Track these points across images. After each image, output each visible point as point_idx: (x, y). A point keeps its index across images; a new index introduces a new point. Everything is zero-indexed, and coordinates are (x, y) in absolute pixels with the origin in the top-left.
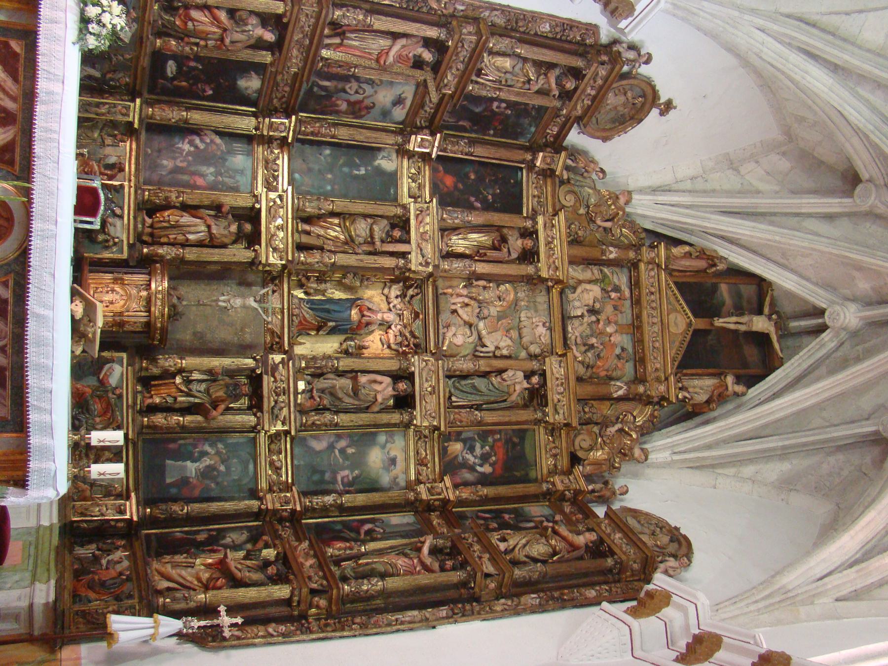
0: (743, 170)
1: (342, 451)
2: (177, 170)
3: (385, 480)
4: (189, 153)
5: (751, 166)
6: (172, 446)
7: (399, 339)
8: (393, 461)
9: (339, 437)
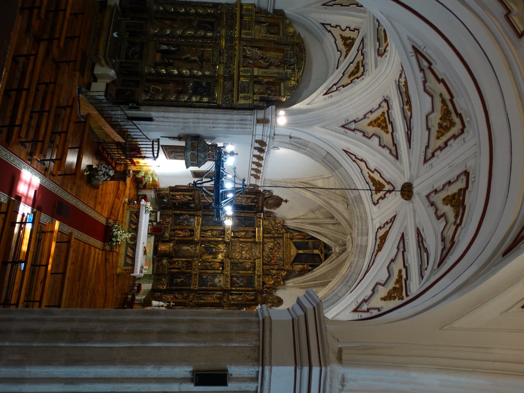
0: (316, 213)
1: (209, 278)
2: (180, 222)
3: (219, 285)
4: (182, 219)
5: (318, 211)
6: (176, 276)
7: (225, 255)
8: (220, 281)
9: (209, 275)
